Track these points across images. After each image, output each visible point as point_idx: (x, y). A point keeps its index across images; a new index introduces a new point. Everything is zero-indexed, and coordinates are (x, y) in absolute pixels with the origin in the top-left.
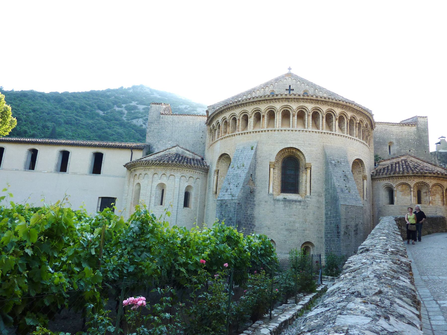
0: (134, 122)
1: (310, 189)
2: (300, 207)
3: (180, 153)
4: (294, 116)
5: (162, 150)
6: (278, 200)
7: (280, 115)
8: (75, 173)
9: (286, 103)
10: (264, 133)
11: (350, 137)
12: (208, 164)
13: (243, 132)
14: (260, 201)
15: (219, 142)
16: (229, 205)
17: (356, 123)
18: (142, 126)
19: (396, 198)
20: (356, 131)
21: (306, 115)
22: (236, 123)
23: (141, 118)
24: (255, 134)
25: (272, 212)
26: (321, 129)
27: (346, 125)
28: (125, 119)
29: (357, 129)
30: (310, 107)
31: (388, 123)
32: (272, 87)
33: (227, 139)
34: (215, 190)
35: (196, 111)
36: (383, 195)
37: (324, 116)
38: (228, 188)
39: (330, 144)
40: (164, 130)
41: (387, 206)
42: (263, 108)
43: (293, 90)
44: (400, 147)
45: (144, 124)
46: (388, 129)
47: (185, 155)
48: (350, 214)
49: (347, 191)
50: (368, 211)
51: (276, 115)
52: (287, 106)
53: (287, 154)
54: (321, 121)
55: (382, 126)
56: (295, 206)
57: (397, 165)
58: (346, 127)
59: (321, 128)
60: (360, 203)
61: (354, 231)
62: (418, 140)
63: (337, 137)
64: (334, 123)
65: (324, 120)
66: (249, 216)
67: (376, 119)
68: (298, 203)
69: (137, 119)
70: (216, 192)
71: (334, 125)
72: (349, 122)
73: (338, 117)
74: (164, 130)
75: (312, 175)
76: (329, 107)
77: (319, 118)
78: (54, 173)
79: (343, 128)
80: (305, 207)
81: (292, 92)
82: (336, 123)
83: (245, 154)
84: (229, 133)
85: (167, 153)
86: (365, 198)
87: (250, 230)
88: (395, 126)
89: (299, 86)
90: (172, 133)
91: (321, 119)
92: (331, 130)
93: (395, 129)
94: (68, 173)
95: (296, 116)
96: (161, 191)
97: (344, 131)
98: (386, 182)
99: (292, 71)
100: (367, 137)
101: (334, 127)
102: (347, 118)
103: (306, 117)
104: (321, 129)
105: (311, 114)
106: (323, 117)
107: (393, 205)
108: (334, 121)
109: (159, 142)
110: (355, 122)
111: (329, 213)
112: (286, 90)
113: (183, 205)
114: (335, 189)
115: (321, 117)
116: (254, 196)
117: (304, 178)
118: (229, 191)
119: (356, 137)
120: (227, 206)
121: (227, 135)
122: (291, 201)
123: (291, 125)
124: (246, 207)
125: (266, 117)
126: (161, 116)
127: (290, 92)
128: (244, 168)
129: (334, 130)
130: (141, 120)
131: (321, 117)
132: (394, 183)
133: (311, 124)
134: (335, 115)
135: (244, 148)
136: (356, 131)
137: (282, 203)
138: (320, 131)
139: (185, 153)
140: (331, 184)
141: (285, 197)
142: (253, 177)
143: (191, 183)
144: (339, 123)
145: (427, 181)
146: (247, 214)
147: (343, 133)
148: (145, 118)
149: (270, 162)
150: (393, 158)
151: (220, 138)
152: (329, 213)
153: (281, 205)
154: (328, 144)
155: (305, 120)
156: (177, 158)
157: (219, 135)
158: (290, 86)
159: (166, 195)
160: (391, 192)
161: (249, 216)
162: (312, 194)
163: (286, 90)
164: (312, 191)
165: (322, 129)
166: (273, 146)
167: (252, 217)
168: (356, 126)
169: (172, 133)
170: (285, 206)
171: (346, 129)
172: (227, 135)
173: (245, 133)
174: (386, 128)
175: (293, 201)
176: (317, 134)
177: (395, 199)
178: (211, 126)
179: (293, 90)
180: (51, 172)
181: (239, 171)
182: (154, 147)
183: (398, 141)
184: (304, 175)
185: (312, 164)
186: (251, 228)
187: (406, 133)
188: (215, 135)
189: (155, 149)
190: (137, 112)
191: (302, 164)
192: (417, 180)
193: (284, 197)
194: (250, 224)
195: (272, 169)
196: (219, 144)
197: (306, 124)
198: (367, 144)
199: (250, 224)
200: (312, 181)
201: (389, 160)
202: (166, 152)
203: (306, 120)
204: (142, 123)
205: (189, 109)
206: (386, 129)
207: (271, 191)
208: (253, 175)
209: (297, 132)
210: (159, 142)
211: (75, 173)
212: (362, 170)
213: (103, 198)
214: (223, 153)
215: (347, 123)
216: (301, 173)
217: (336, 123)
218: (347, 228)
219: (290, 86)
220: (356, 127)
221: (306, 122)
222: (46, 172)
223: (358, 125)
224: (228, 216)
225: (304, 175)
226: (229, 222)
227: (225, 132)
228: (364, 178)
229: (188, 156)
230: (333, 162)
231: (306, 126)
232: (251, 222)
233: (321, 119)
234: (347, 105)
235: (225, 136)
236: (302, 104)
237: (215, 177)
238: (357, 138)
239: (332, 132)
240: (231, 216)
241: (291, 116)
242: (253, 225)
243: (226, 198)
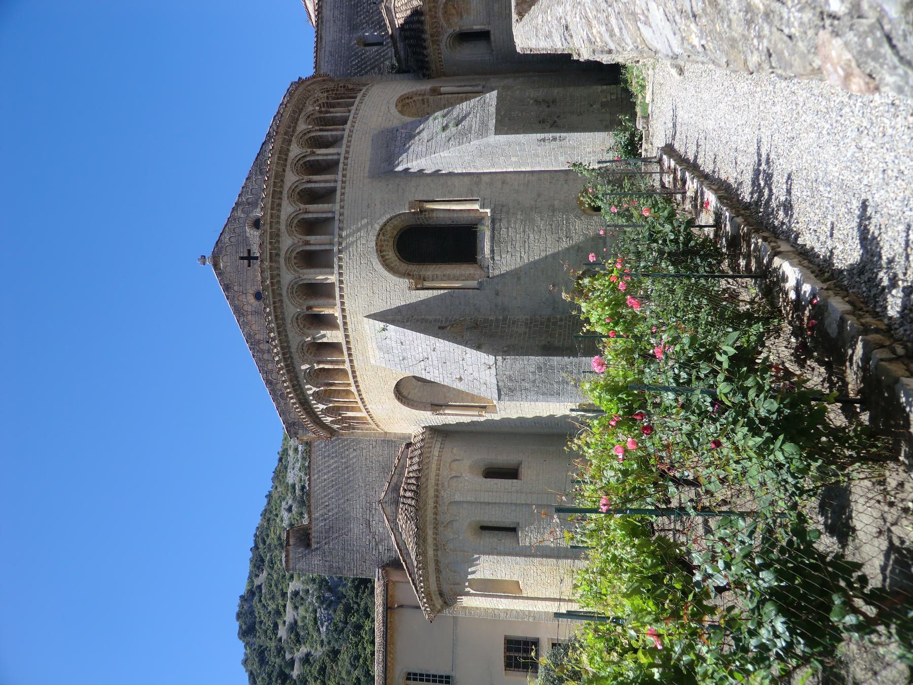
4: (307, 243)
7: (305, 271)
10: (346, 306)
11: (349, 122)
12: (421, 430)
13: (345, 353)
14: (496, 306)
15: (368, 406)
17: (320, 112)
19: (475, 27)
20: (338, 112)
21: (306, 216)
22: (324, 369)
23: (316, 611)
24: (349, 327)
25: (519, 278)
29: (331, 110)
31: (316, 52)
33: (361, 388)
35: (294, 486)
36: (471, 53)
37: (306, 178)
39: (368, 163)
41: (493, 44)
42: (292, 309)
46: (328, 49)
50: (506, 81)
51: (306, 282)
52: (288, 260)
53: (391, 255)
54: (317, 185)
55: (322, 63)
58: (329, 133)
59: (332, 185)
60: (492, 97)
61: (548, 107)
64: (320, 158)
65: (315, 178)
66: (530, 328)
67: (308, 71)
68: (497, 226)
70: (484, 407)
71: (325, 158)
72: (317, 128)
73: (309, 150)
76: (288, 169)
77: (310, 189)
79: (330, 139)
83: (394, 345)
84: (349, 385)
86: (480, 88)
87: (560, 326)
88: (324, 37)
91: (313, 185)
92: (337, 163)
93: (329, 36)
95: (308, 238)
96: (484, 532)
97: (337, 136)
98: (443, 46)
99: (209, 254)
100: (348, 90)
101: (330, 157)
102: (309, 132)
103: (310, 216)
105: (302, 206)
106: (309, 182)
107: (492, 32)
108: (317, 158)
110: (318, 115)
111: (513, 159)
113: (515, 481)
115: (309, 185)
116: (486, 321)
117: (441, 215)
119: (349, 111)
121: (353, 388)
123: (328, 247)
124: (511, 336)
125: (311, 303)
126: (314, 546)
127: (256, 258)
129: (335, 157)
131: (309, 185)
133: (326, 205)
134: (305, 156)
136: (338, 112)
142: (444, 325)
144: (320, 147)
146: (525, 333)
147: (342, 137)
151: (360, 404)
154: (367, 169)
155: (317, 219)
156: (409, 501)
157: (353, 409)
158: (242, 258)
159: (493, 519)
160: (466, 37)
161: (530, 328)
163: (249, 266)
167: (531, 323)
168: (327, 112)
171: (334, 133)
172: (353, 388)
173: (349, 349)
174: (327, 53)
176: (347, 190)
177: (477, 27)
178: (336, 426)
184: (434, 215)
185: (411, 199)
186: (555, 324)
187: (337, 13)
188: (354, 418)
191: (412, 222)
194: (547, 326)
195: (427, 284)
196: (374, 407)
197: (324, 215)
198: (364, 89)
199: (547, 326)
203: (315, 215)
205: (290, 502)
206: (330, 52)
207: (474, 284)
208: (439, 324)
212: (420, 98)
215: (321, 130)
216: (430, 222)
217: (323, 153)
218: (543, 122)
219: (242, 258)
220: (329, 112)
221: (320, 215)
223: (323, 109)
225: (434, 215)
227: (348, 392)
228: (435, 91)
231: (330, 215)
232: (542, 323)
233: (313, 185)
234: (283, 130)
235: (356, 393)
236: (283, 227)
237: (446, 412)
238: (354, 108)
239: (342, 160)
241: (308, 248)
242: (549, 319)
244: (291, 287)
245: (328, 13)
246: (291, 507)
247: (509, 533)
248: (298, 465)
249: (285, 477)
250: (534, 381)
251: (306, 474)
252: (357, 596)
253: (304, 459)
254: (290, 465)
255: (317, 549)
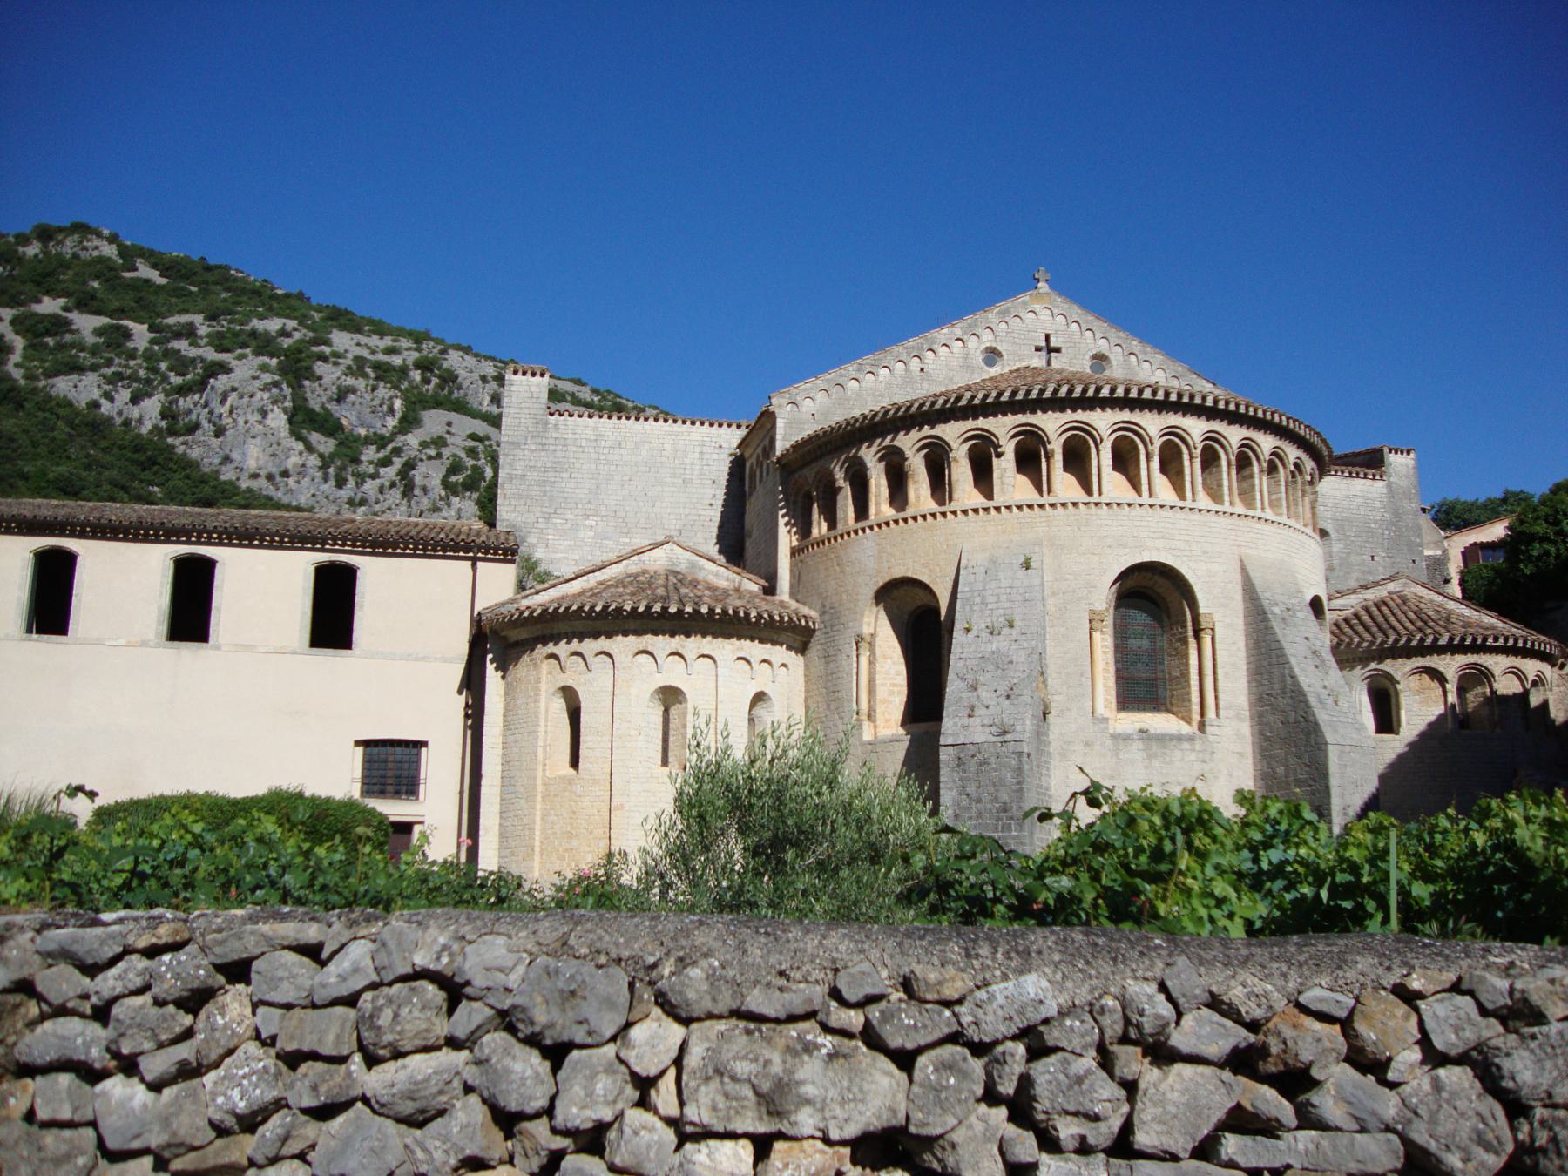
0: (63, 386)
1: (1216, 698)
2: (1193, 756)
3: (682, 568)
5: (612, 556)
6: (1127, 738)
8: (249, 648)
9: (1126, 415)
16: (993, 760)
18: (95, 405)
23: (94, 368)
26: (1227, 503)
27: (1283, 488)
28: (17, 374)
30: (1196, 428)
32: (991, 337)
34: (864, 706)
35: (327, 343)
37: (1233, 459)
38: (974, 701)
40: (566, 475)
43: (1058, 350)
44: (1346, 546)
45: (109, 396)
47: (700, 576)
48: (1349, 770)
49: (1330, 701)
56: (1178, 754)
57: (1384, 608)
59: (1226, 498)
62: (1392, 524)
63: (1269, 527)
64: (1257, 482)
68: (1186, 745)
69: (75, 377)
74: (566, 475)
75: (1218, 652)
78: (158, 646)
80: (1207, 757)
81: (1058, 362)
82: (1260, 481)
83: (1004, 583)
85: (634, 569)
89: (1077, 339)
90: (598, 486)
94: (218, 648)
101: (1258, 495)
104: (1227, 503)
105: (1199, 451)
108: (1257, 476)
109: (547, 520)
111: (1281, 770)
112: (1038, 349)
114: (1297, 696)
118: (980, 711)
120: (983, 763)
122: (1163, 739)
128: (1014, 631)
130: (91, 379)
132: (1399, 669)
135: (993, 561)
137: (1140, 745)
138: (1226, 507)
139: (701, 568)
140: (1283, 681)
141: (1145, 726)
143: (762, 680)
145: (1488, 660)
147: (1280, 515)
148: (108, 371)
149: (1092, 612)
150: (1365, 587)
152: (1281, 770)
153: (1135, 751)
158: (1047, 337)
162: (1222, 712)
163: (1038, 349)
164: (1221, 703)
165: (1232, 503)
166: (1096, 558)
169: (598, 486)
170: (1150, 757)
175: (1172, 738)
179: (1058, 350)
180: (144, 644)
181: (1000, 644)
182: (532, 540)
183: (1340, 524)
185: (1216, 617)
187: (1360, 500)
189: (534, 546)
190: (73, 345)
192: (1461, 660)
193: (1138, 726)
200: (1219, 671)
201: (1354, 592)
202: (632, 566)
204: (96, 394)
205: (297, 335)
209: (1167, 513)
210: (547, 520)
211: (249, 648)
213: (366, 744)
214: (899, 572)
219: (1047, 337)
222: (122, 642)
224: (996, 800)
226: (999, 819)
229: (711, 578)
230: (1277, 610)
237: (864, 661)
239: (1251, 513)
240: (1004, 797)
243: (980, 737)
244: (1085, 428)
245: (1358, 488)
246: (288, 335)
247: (659, 756)
248: (365, 353)
249: (343, 328)
250: (979, 801)
251: (349, 368)
252: (122, 448)
253: (377, 366)
254: (363, 340)
255: (547, 423)
